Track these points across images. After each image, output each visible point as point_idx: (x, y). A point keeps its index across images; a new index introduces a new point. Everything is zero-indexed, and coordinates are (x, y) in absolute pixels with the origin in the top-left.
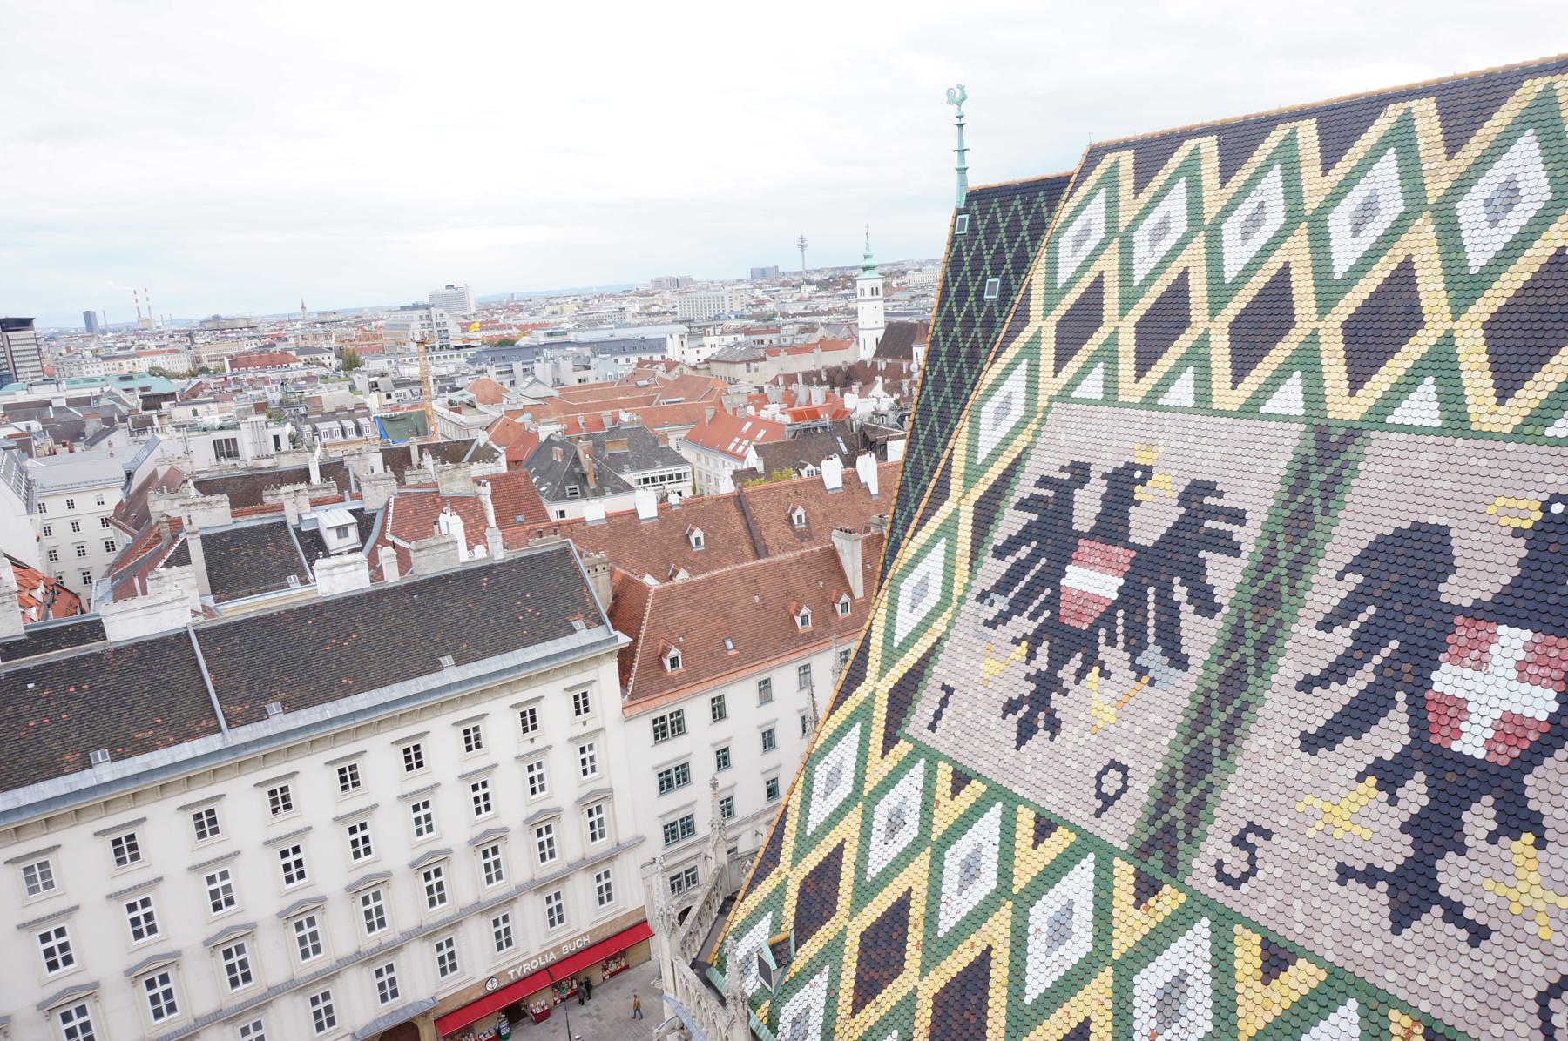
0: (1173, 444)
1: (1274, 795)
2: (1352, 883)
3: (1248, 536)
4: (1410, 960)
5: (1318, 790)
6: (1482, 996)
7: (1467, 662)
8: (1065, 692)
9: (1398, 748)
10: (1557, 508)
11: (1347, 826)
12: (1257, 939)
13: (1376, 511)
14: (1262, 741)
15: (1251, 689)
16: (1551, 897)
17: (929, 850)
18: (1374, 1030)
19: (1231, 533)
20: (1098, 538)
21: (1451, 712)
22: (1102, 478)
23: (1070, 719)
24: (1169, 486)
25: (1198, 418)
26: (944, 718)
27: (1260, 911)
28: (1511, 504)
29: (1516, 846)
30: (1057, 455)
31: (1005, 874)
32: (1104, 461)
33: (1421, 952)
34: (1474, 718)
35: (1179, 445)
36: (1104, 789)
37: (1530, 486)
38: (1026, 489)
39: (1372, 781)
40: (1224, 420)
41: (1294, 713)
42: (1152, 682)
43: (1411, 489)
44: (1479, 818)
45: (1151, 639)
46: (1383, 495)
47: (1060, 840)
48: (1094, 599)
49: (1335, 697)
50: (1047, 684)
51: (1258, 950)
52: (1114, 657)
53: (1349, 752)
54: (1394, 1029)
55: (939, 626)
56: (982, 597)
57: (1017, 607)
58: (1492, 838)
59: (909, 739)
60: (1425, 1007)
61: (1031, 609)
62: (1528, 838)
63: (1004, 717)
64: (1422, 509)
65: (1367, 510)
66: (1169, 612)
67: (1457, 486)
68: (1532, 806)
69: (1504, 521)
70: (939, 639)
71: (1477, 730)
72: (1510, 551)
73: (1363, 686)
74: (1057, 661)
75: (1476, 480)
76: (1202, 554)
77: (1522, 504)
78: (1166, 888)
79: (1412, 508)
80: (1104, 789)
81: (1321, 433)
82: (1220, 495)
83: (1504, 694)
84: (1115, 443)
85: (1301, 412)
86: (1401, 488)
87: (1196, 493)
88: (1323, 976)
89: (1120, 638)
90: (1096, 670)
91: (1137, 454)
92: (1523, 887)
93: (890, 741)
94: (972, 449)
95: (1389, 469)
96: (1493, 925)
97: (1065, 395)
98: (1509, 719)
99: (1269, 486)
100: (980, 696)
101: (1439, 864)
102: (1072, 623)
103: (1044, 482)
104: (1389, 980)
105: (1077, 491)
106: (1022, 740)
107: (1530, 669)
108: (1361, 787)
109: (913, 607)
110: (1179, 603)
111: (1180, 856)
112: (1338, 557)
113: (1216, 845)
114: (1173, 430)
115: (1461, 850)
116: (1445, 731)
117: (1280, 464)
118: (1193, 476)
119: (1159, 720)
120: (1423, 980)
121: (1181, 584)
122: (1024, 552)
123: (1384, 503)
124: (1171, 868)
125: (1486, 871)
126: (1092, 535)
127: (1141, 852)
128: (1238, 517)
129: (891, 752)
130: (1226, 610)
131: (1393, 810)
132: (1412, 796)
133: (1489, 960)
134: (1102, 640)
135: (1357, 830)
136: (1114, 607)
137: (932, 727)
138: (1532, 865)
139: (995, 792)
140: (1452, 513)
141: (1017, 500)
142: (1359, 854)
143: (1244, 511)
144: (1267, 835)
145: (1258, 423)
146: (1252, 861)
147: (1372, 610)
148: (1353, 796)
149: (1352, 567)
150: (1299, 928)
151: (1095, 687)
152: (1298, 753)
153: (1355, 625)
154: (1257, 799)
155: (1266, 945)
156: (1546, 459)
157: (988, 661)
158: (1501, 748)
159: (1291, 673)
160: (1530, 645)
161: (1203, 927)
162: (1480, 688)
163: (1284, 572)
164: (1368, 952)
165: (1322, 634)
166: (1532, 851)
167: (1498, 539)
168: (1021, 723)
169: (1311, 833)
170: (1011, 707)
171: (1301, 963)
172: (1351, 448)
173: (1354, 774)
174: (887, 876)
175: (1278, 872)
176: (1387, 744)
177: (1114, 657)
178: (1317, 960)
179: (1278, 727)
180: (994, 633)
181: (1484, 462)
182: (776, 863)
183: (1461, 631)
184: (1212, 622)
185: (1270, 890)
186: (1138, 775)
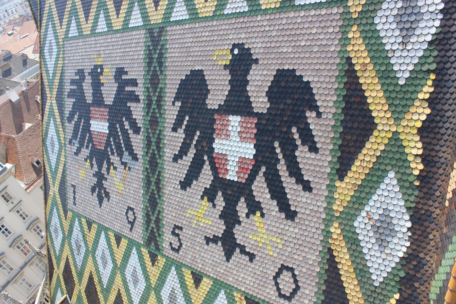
2: (210, 243)
3: (140, 91)
6: (258, 282)
7: (223, 136)
10: (236, 52)
11: (203, 221)
15: (160, 166)
18: (231, 301)
22: (89, 75)
23: (111, 192)
26: (77, 200)
27: (187, 260)
29: (256, 219)
31: (114, 261)
33: (237, 269)
34: (231, 163)
38: (68, 87)
39: (206, 198)
42: (129, 168)
45: (124, 149)
47: (124, 243)
49: (186, 163)
50: (100, 177)
51: (191, 277)
52: (115, 159)
54: (237, 299)
55: (62, 159)
56: (70, 142)
58: (248, 216)
60: (243, 289)
62: (258, 214)
63: (92, 194)
68: (257, 200)
69: (220, 63)
70: (64, 164)
73: (193, 156)
74: (100, 167)
78: (159, 258)
80: (130, 220)
82: (126, 73)
87: (120, 72)
89: (115, 151)
90: (112, 167)
93: (66, 212)
96: (255, 253)
98: (242, 161)
102: (99, 148)
103: (73, 82)
106: (101, 203)
107: (244, 135)
110: (127, 129)
115: (239, 223)
116: (223, 171)
117: (141, 53)
121: (126, 120)
122: (76, 117)
124: (158, 249)
126: (93, 105)
128: (134, 83)
129: (68, 218)
130: (142, 130)
131: (216, 212)
132: (220, 203)
133: (257, 267)
134: (110, 153)
136: (109, 135)
137: (75, 204)
139: (101, 228)
141: (67, 93)
142: (210, 232)
143: (136, 80)
144: (181, 228)
146: (180, 240)
147: (187, 118)
149: (177, 99)
150: (200, 266)
153: (184, 127)
154: (174, 215)
156: (227, 27)
158: (242, 175)
161: (173, 271)
163: (155, 107)
165: (175, 134)
166: (261, 220)
168: (98, 195)
170: (93, 190)
172: (162, 38)
173: (199, 197)
177: (115, 159)
178: (209, 277)
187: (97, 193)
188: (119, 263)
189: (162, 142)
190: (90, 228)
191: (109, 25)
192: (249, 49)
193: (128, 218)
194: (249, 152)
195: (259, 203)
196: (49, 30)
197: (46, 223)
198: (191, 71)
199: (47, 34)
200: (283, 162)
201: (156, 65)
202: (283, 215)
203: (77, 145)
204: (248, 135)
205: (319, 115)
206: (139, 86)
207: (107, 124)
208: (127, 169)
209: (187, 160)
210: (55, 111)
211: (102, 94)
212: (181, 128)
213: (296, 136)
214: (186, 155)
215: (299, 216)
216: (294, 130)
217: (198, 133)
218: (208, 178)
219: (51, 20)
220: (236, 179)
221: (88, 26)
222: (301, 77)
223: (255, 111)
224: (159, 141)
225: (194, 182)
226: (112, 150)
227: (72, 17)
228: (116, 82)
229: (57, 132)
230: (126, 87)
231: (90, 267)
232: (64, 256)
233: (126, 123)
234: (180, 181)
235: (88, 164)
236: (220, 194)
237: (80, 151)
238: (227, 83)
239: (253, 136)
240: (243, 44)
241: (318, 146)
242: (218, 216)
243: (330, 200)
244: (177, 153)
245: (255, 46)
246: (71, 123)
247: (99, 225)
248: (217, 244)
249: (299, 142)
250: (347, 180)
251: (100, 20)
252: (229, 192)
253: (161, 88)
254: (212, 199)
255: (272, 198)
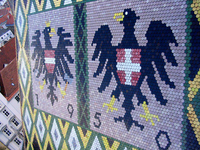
0: (52, 19)
1: (98, 105)
2: (117, 121)
3: (72, 39)
4: (132, 137)
5: (105, 101)
8: (55, 90)
9: (116, 87)
10: (126, 13)
11: (113, 108)
12: (106, 138)
13: (93, 25)
14: (92, 92)
16: (152, 115)
17: (48, 132)
19: (69, 40)
20: (47, 49)
21: (122, 75)
24: (55, 31)
25: (54, 11)
26: (39, 102)
27: (104, 132)
28: (118, 15)
29: (143, 105)
30: (33, 30)
31: (62, 135)
32: (42, 30)
35: (53, 19)
36: (70, 111)
37: (120, 8)
39: (114, 96)
40: (58, 10)
41: (95, 83)
43: (98, 17)
44: (135, 100)
45: (65, 72)
46: (93, 20)
47: (67, 125)
48: (52, 65)
50: (52, 88)
51: (107, 141)
52: (60, 78)
53: (108, 90)
55: (30, 80)
56: (34, 71)
57: (40, 72)
58: (138, 104)
59: (36, 108)
60: (138, 146)
61: (43, 71)
62: (145, 102)
64: (101, 22)
65: (92, 25)
66: (65, 63)
67: (106, 13)
69: (118, 20)
71: (128, 78)
72: (121, 28)
73: (105, 73)
74: (51, 83)
75: (109, 10)
76: (66, 47)
77: (120, 14)
78: (88, 131)
79: (100, 22)
81: (76, 6)
82: (64, 30)
83: (130, 67)
84: (42, 23)
85: (71, 2)
86: (96, 17)
87: (60, 30)
88: (119, 143)
89: (59, 73)
90: (58, 83)
91: (46, 24)
92: (147, 115)
93: (33, 110)
94: (19, 33)
95: (92, 13)
97: (29, 14)
98: (134, 73)
99: (72, 25)
100: (42, 95)
101: (131, 113)
103: (34, 38)
104: (130, 142)
105: (40, 38)
106: (53, 104)
108: (112, 98)
109: (24, 77)
111: (87, 123)
112: (90, 40)
113: (92, 120)
114: (50, 16)
115: (134, 109)
118: (58, 27)
119: (73, 92)
120: (136, 140)
121: (65, 56)
123: (94, 22)
124: (87, 126)
125: (140, 112)
126: (45, 49)
127: (81, 124)
128: (69, 35)
130: (75, 60)
134: (57, 75)
135: (115, 109)
136: (56, 65)
137: (38, 105)
138: (147, 109)
139: (53, 117)
140: (107, 21)
145: (65, 8)
146: (99, 121)
147: (100, 52)
148: (112, 101)
149: (94, 42)
150: (112, 134)
151: (60, 87)
152: (99, 93)
153: (99, 57)
154: (96, 106)
155: (108, 139)
157: (40, 86)
158: (134, 81)
159: (91, 73)
160: (132, 53)
162: (126, 67)
164: (125, 136)
165: (93, 61)
166: (146, 105)
167: (118, 25)
169: (107, 112)
170: (48, 96)
171: (115, 141)
172: (84, 9)
174: (44, 139)
175: (105, 123)
176: (113, 86)
177: (60, 78)
179: (93, 88)
180: (39, 79)
181: (109, 5)
182: (27, 141)
183: (118, 53)
184: (73, 64)
185: (105, 127)
186: (74, 106)
187: (50, 97)
188: (65, 135)
189: (87, 66)
190: (47, 118)
191: (53, 4)
192: (134, 11)
193: (69, 110)
194: (138, 68)
195: (145, 96)
196: (19, 10)
197: (22, 116)
198: (101, 26)
199: (18, 13)
200: (157, 72)
201: (81, 24)
202: (159, 102)
203: (38, 72)
204: (136, 59)
205: (177, 45)
206: (72, 36)
207: (55, 59)
208: (67, 83)
209: (102, 75)
210: (24, 54)
211: (51, 43)
212: (97, 58)
213: (164, 57)
214: (101, 73)
215: (168, 102)
216: (163, 54)
217: (107, 60)
218: (114, 84)
219: (20, 5)
220: (130, 84)
221: (41, 6)
222: (165, 24)
223: (140, 45)
224: (85, 66)
225: (107, 87)
226: (58, 74)
227: (32, 2)
228: (58, 36)
229: (26, 65)
230: (64, 38)
231: (48, 139)
232: (33, 134)
233: (65, 58)
234: (98, 88)
235: (44, 82)
236: (122, 93)
237: (40, 75)
238: (122, 31)
239: (139, 59)
240: (130, 9)
241: (177, 62)
242: (121, 106)
243: (186, 92)
244: (96, 72)
245: (137, 9)
246: (34, 60)
247: (52, 115)
248: (121, 121)
249: (166, 61)
250: (195, 80)
251: (47, 2)
252: (127, 91)
253: (84, 37)
254: (117, 96)
255: (152, 93)
